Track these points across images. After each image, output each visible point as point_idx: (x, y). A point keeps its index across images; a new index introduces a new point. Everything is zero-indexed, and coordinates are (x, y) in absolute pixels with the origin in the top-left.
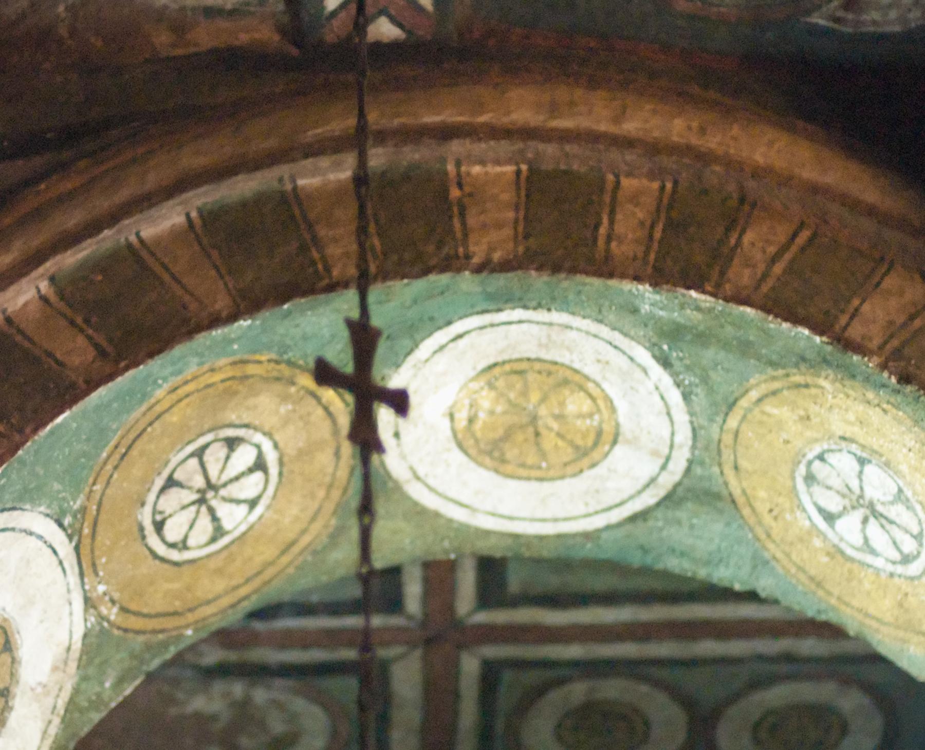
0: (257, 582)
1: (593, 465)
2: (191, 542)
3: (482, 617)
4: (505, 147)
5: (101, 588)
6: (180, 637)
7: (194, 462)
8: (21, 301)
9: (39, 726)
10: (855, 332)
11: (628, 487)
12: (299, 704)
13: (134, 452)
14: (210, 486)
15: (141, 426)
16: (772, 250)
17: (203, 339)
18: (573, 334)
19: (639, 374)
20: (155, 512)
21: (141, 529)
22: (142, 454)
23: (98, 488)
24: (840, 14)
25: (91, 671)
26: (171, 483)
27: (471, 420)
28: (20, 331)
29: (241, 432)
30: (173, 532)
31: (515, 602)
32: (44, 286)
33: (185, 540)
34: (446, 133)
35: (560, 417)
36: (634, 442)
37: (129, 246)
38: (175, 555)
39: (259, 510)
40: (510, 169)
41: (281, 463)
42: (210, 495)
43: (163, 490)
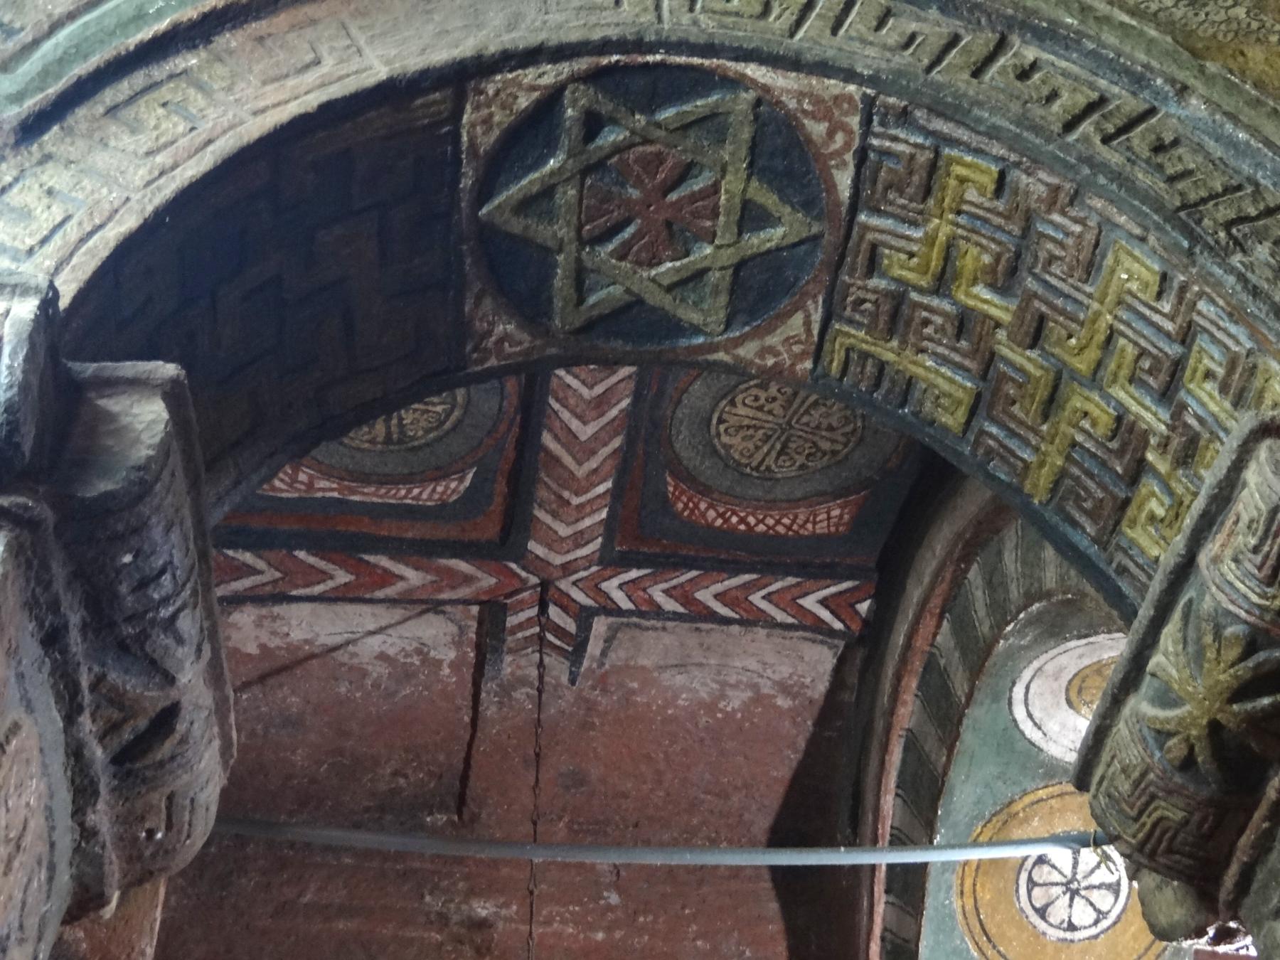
13: (992, 931)
14: (1067, 884)
20: (1058, 927)
26: (1042, 912)
33: (1099, 912)
38: (1105, 924)
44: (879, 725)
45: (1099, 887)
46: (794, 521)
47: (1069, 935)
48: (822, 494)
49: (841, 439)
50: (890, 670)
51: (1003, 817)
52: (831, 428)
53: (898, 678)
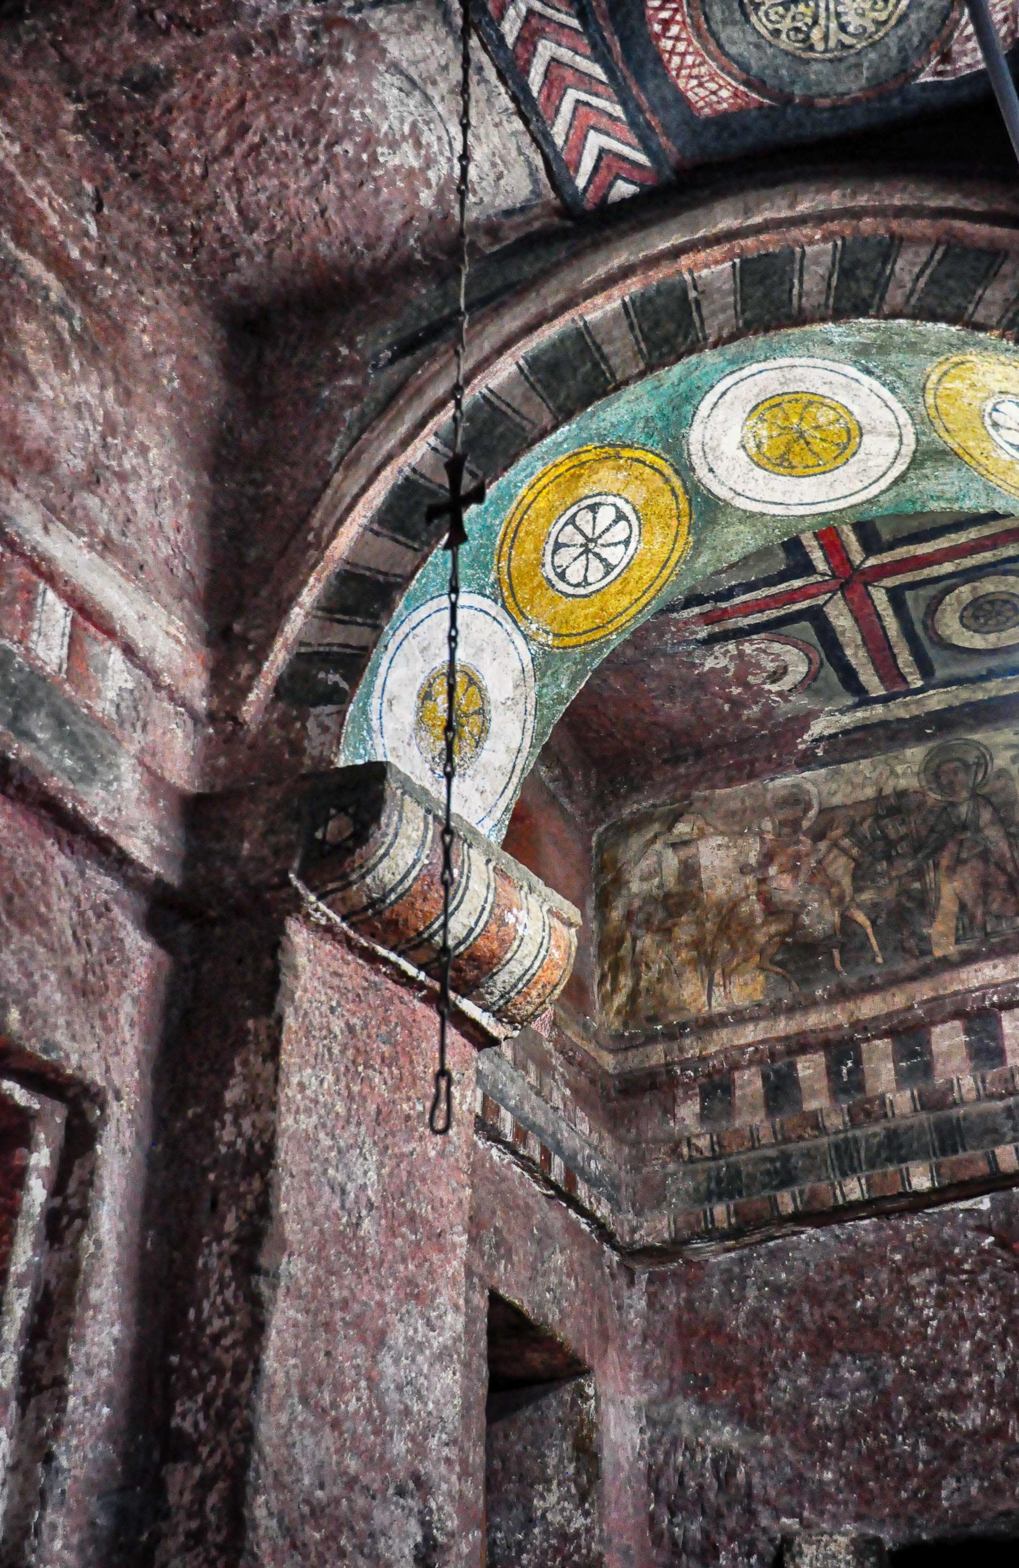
0: (652, 592)
1: (854, 454)
2: (590, 580)
3: (872, 562)
4: (717, 251)
5: (534, 627)
6: (608, 642)
7: (570, 527)
8: (419, 455)
9: (518, 725)
10: (979, 317)
11: (885, 463)
12: (776, 647)
13: (521, 534)
15: (518, 516)
16: (917, 270)
17: (538, 449)
18: (798, 371)
19: (854, 384)
20: (554, 568)
21: (549, 581)
22: (527, 533)
23: (503, 564)
24: (940, 68)
25: (546, 680)
26: (558, 546)
27: (759, 446)
28: (422, 476)
29: (597, 499)
30: (574, 575)
31: (891, 546)
32: (432, 440)
34: (676, 253)
35: (817, 427)
36: (873, 431)
37: (484, 397)
38: (581, 591)
39: (633, 545)
40: (728, 264)
41: (636, 511)
42: (591, 546)
43: (554, 552)
44: (552, 293)
45: (602, 560)
46: (694, 66)
47: (555, 579)
48: (745, 68)
49: (832, 43)
50: (620, 259)
51: (611, 451)
52: (843, 28)
53: (626, 272)
